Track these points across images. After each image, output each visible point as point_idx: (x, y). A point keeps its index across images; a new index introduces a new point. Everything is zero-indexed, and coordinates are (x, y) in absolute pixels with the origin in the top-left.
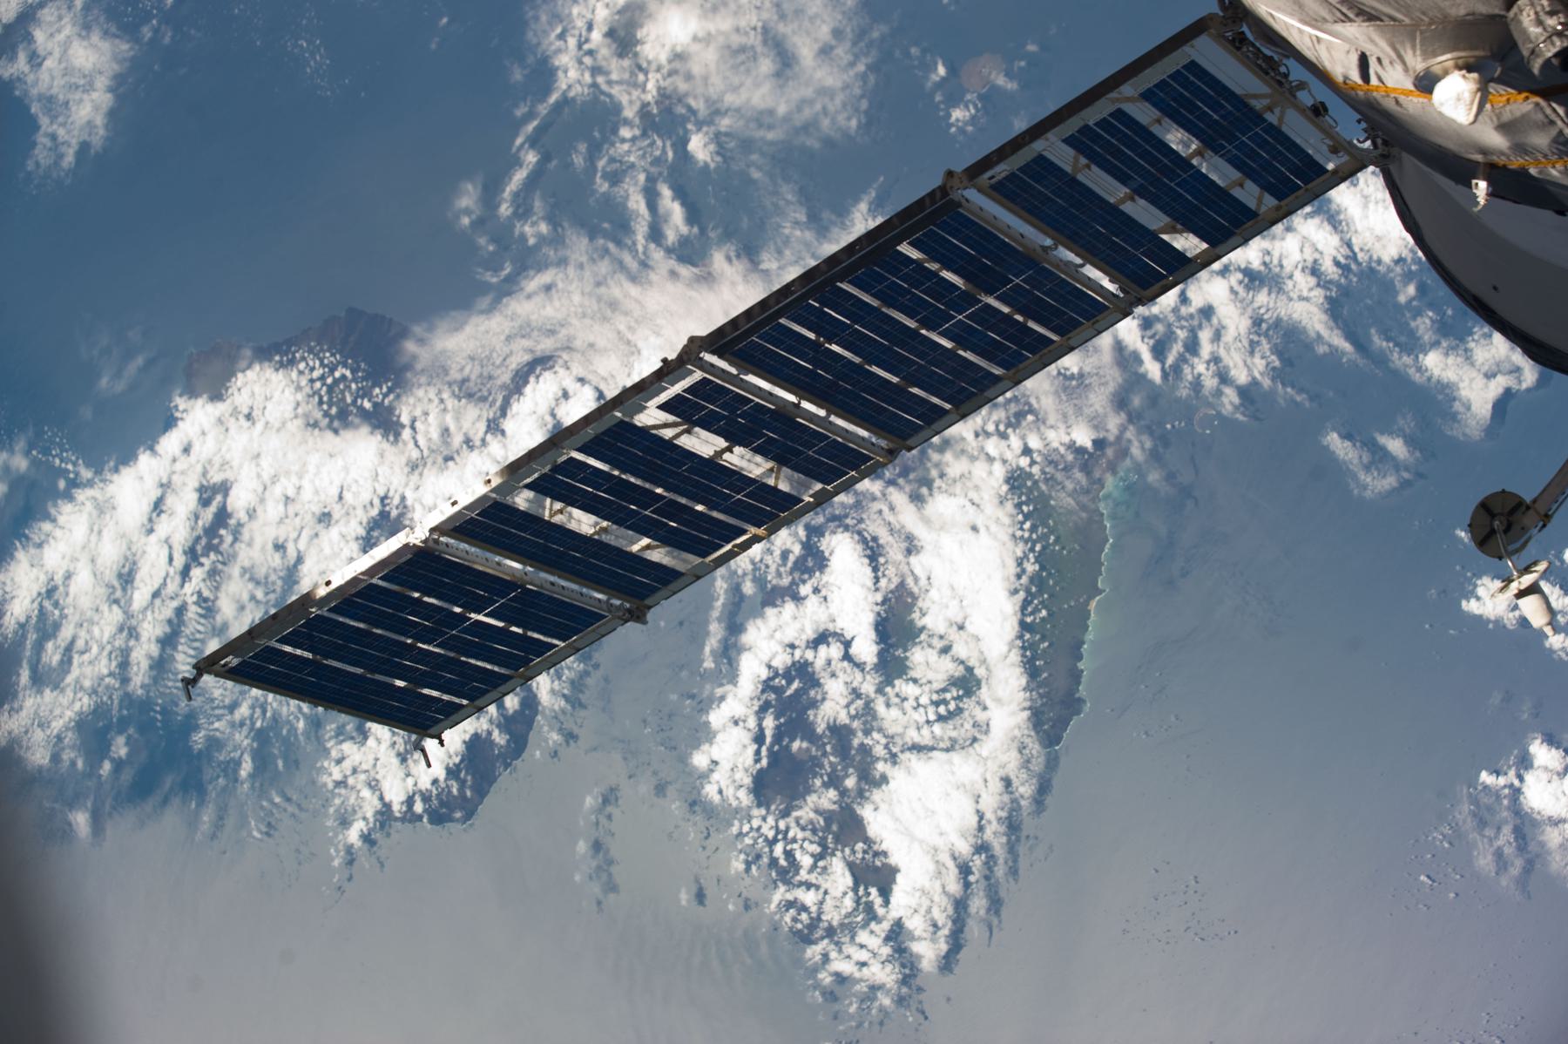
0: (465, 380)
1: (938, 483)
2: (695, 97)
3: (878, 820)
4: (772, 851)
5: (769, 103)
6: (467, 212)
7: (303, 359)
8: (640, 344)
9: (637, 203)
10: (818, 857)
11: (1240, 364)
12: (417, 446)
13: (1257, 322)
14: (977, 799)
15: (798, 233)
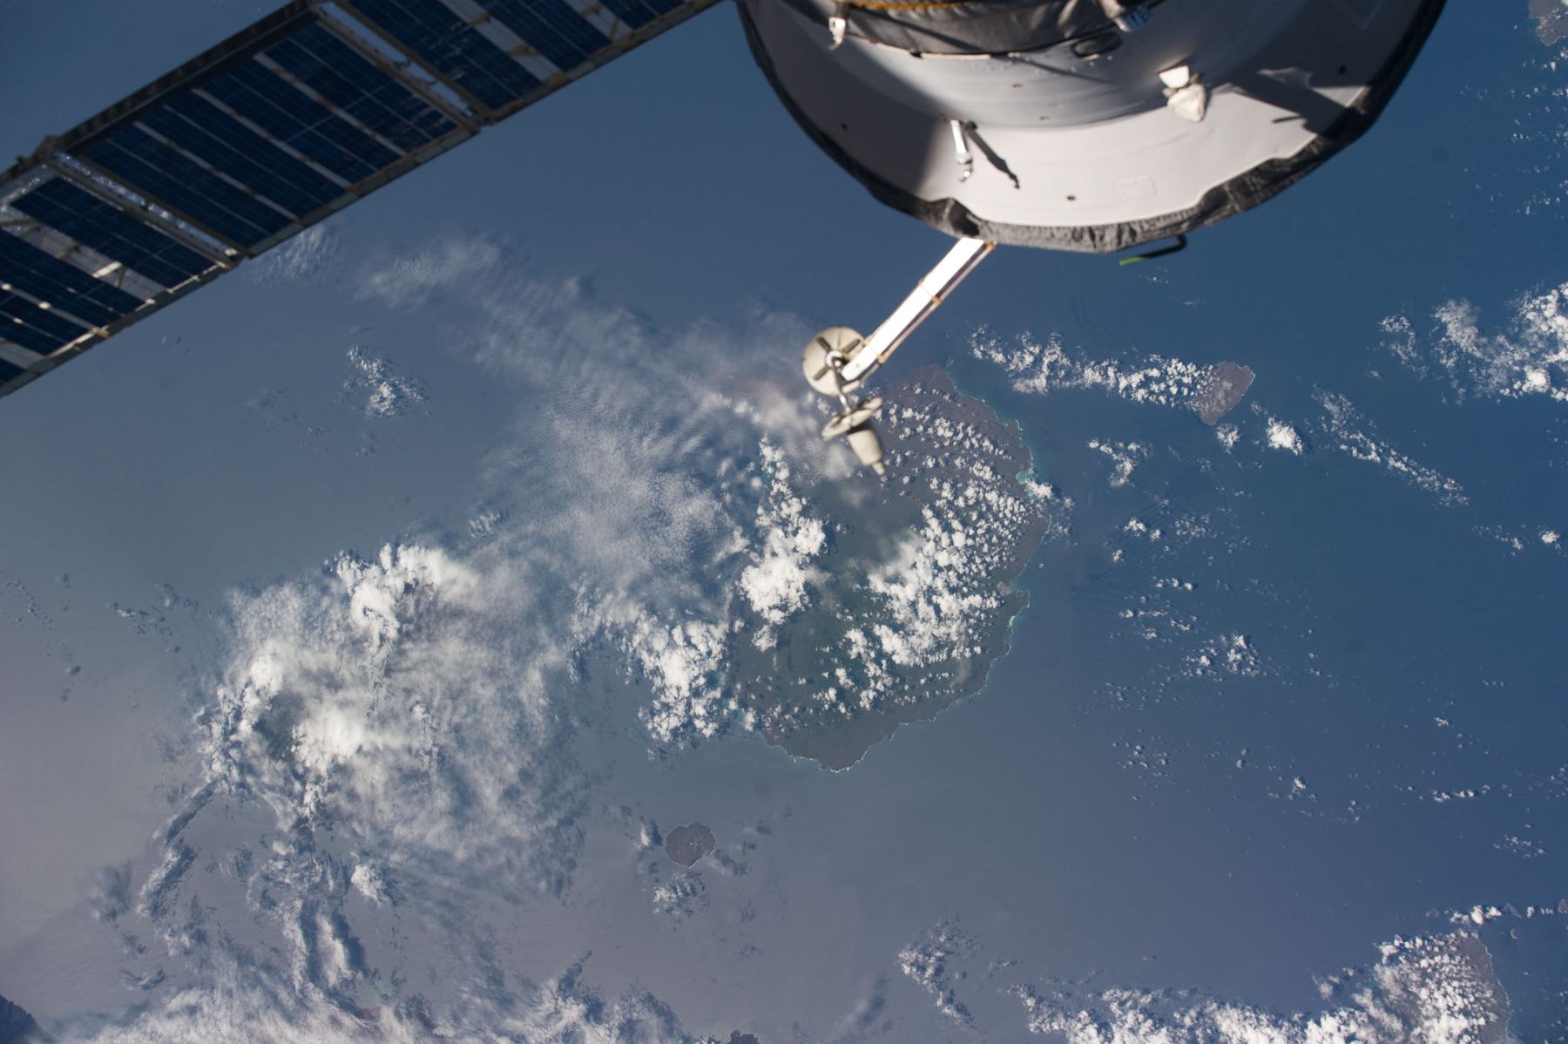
2: (360, 822)
5: (445, 844)
6: (95, 903)
9: (293, 932)
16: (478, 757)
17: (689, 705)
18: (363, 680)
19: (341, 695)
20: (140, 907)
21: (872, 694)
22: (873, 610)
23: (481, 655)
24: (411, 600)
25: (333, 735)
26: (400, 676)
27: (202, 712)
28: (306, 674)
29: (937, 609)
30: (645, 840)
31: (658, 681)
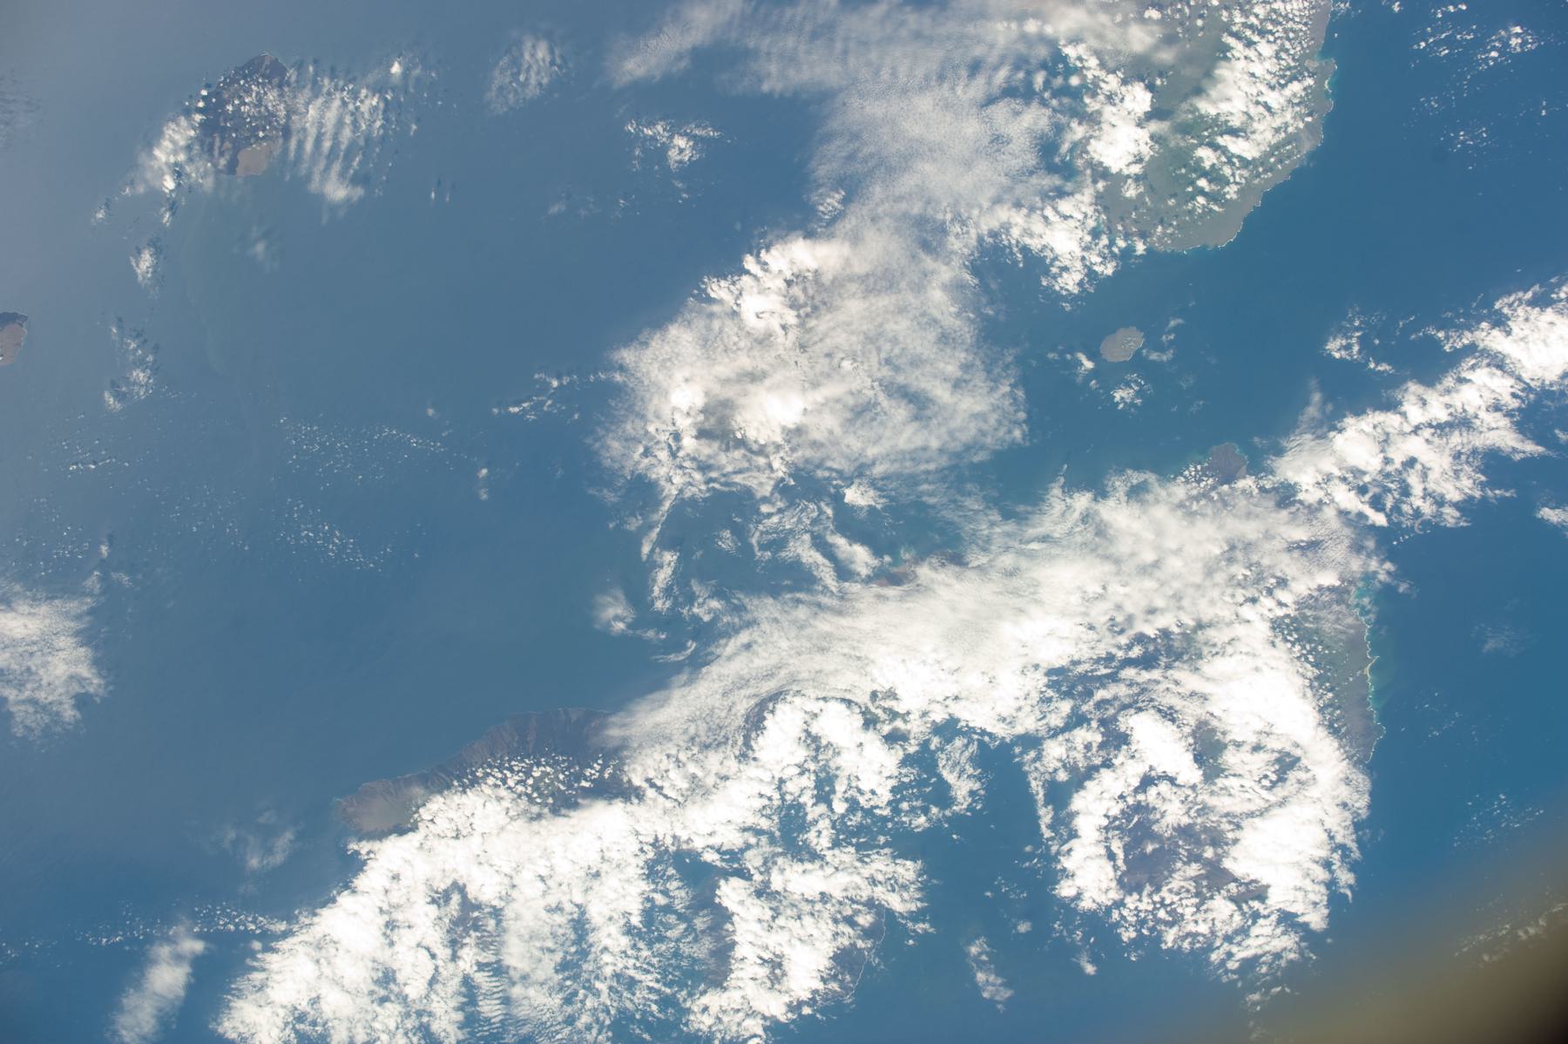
0: (693, 739)
1: (1205, 650)
3: (1240, 863)
4: (1155, 916)
5: (919, 441)
7: (488, 775)
8: (872, 656)
9: (810, 556)
10: (1198, 907)
11: (1452, 489)
12: (666, 797)
13: (1457, 456)
14: (1322, 822)
15: (998, 530)
16: (918, 373)
17: (1083, 258)
18: (782, 362)
19: (767, 382)
20: (659, 604)
21: (1235, 188)
22: (1212, 130)
23: (884, 302)
24: (796, 290)
25: (771, 413)
26: (817, 347)
27: (641, 450)
28: (725, 382)
29: (1268, 108)
30: (1089, 365)
31: (1048, 253)
